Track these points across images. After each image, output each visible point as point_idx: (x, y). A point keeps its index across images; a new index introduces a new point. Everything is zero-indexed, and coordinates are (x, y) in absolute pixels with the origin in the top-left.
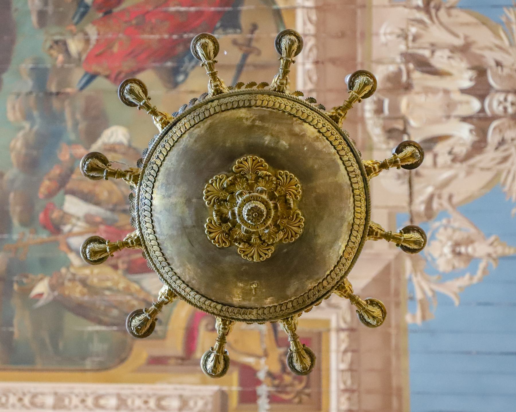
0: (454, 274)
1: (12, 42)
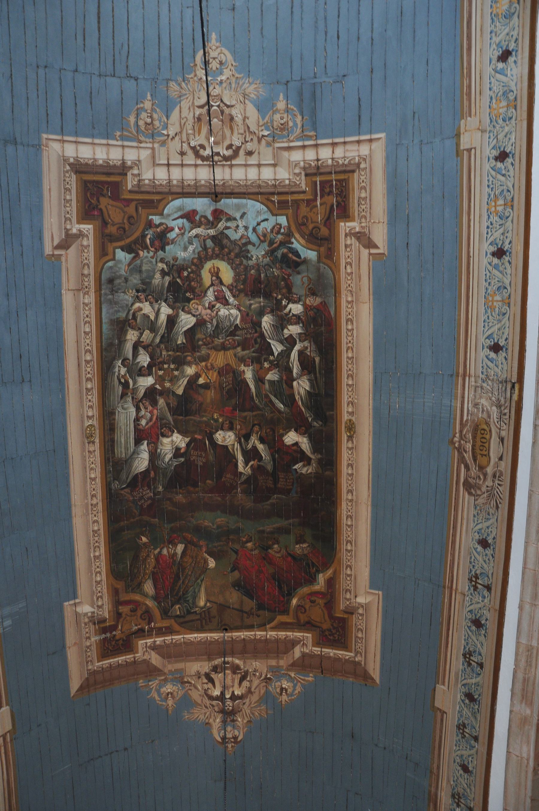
0: (159, 694)
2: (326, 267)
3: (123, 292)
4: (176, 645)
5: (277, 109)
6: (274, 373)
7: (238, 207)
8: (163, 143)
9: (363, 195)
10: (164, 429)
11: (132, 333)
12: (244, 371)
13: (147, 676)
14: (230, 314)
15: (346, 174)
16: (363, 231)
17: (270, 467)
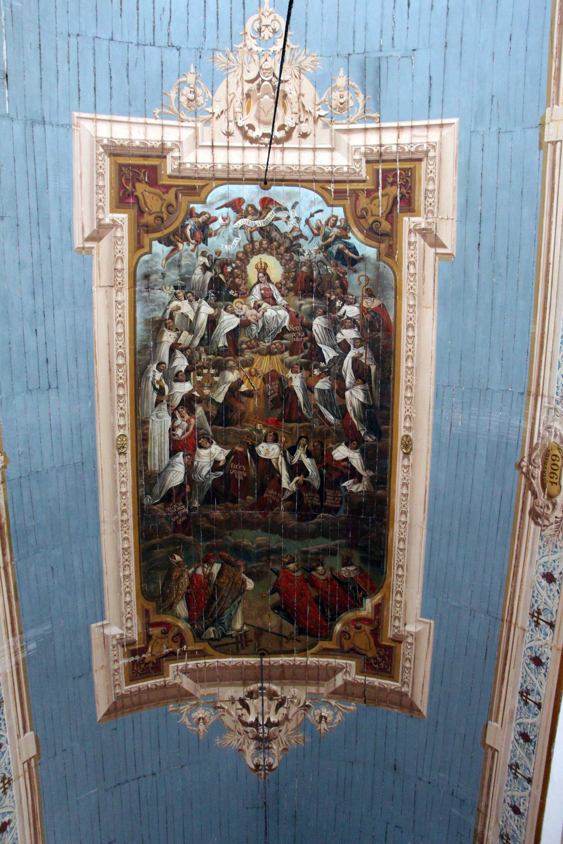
0: (190, 719)
1: (294, 539)
2: (387, 266)
3: (160, 289)
4: (209, 669)
5: (336, 86)
6: (325, 381)
7: (289, 196)
8: (207, 122)
9: (431, 187)
10: (202, 439)
11: (169, 333)
12: (291, 378)
13: (177, 701)
14: (278, 315)
15: (412, 163)
16: (429, 227)
17: (316, 484)
